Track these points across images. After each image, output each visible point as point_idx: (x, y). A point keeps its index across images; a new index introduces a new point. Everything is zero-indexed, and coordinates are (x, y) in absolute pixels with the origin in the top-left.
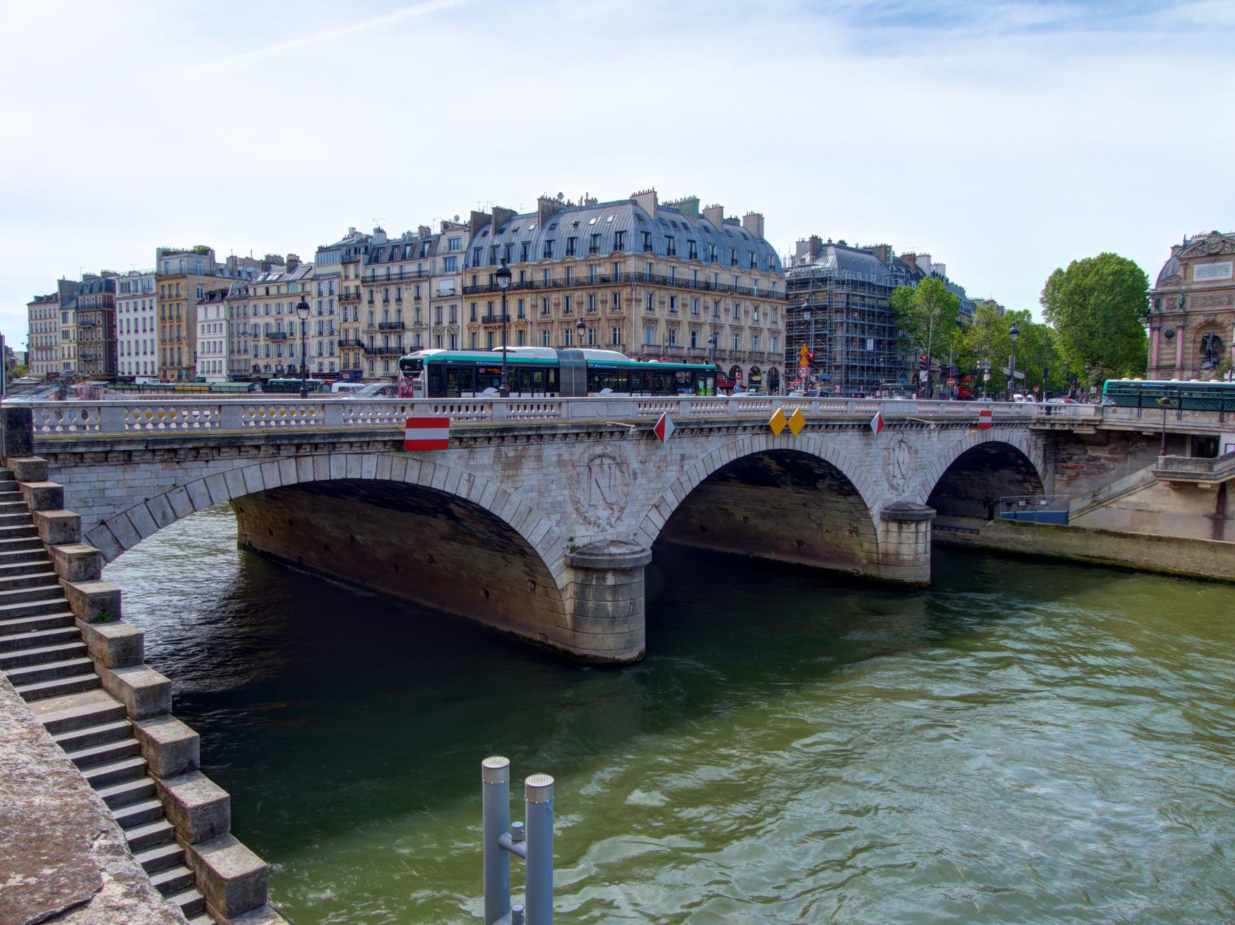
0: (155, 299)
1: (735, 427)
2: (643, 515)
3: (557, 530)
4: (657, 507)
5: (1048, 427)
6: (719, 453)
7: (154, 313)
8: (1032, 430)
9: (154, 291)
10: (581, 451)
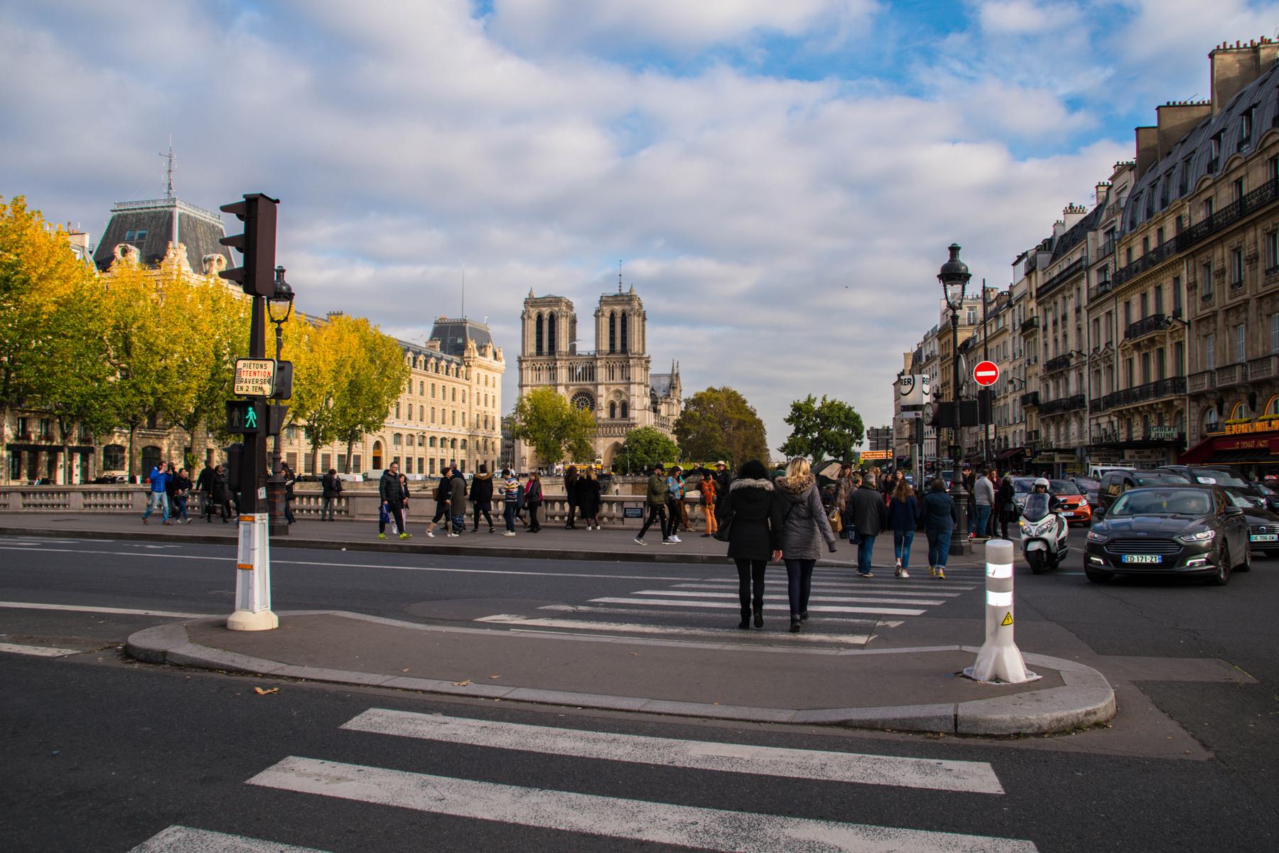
0: (938, 362)
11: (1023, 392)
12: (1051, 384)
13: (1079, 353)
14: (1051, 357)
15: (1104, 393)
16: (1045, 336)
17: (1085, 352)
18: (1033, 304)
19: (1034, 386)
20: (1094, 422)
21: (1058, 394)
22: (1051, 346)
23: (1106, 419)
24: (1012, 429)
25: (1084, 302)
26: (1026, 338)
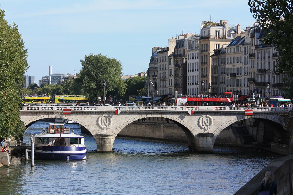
2: (115, 128)
3: (95, 129)
4: (119, 127)
5: (283, 114)
7: (198, 60)
8: (281, 115)
9: (199, 48)
11: (248, 77)
12: (259, 76)
13: (269, 69)
14: (260, 68)
15: (276, 83)
16: (258, 61)
17: (271, 70)
18: (253, 48)
20: (273, 90)
21: (261, 80)
22: (260, 65)
23: (276, 90)
24: (244, 88)
25: (271, 56)
26: (250, 59)
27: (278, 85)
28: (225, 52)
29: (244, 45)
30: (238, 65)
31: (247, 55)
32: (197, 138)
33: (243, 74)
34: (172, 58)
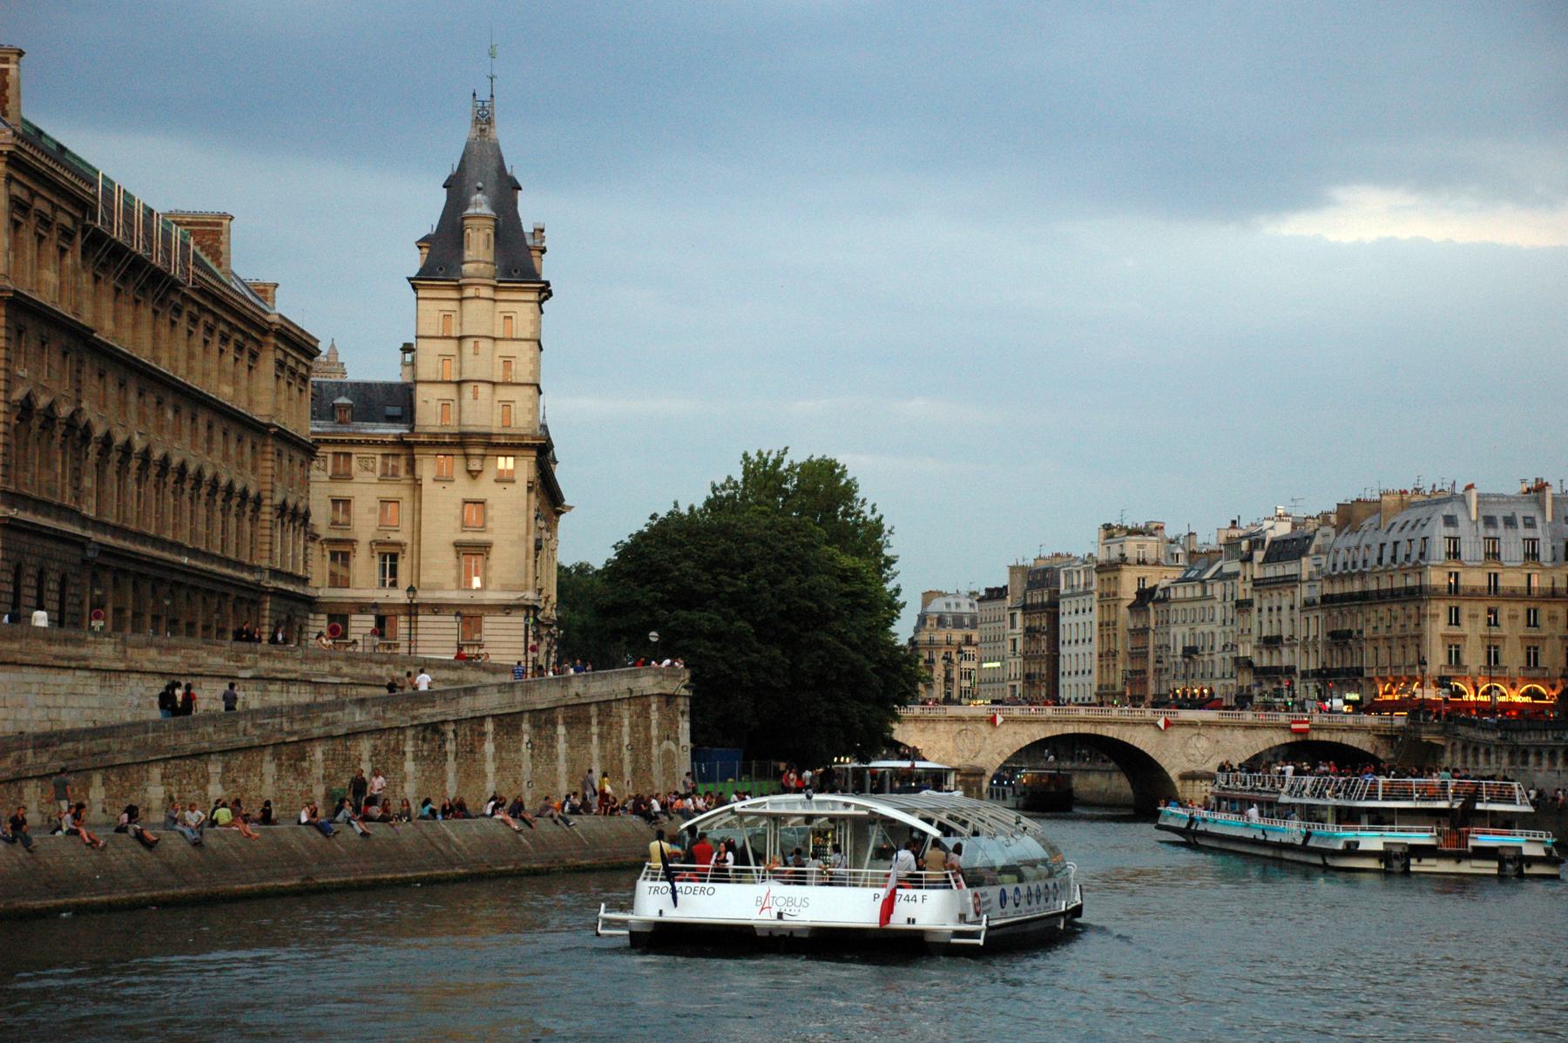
0: (1096, 596)
1: (1047, 721)
6: (1039, 733)
7: (1094, 617)
10: (957, 727)
18: (1249, 586)
19: (1246, 650)
25: (1298, 605)
27: (1317, 674)
28: (1165, 600)
29: (1221, 579)
30: (1206, 628)
31: (1230, 604)
32: (1178, 784)
33: (1218, 648)
34: (1019, 613)
